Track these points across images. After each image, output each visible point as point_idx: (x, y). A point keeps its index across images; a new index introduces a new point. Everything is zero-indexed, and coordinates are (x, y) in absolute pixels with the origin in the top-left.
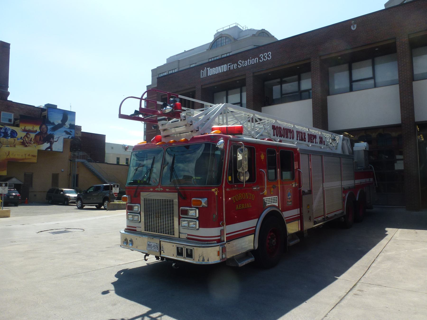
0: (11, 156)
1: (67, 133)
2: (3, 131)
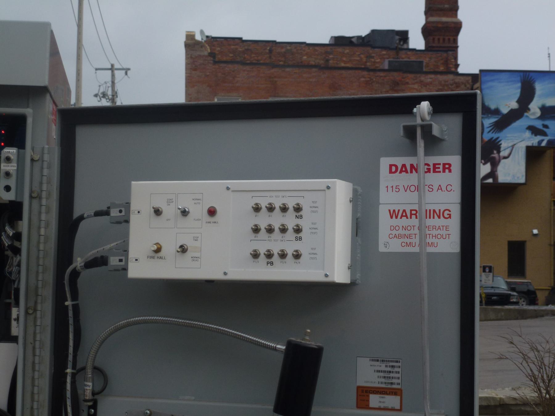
1: (534, 131)
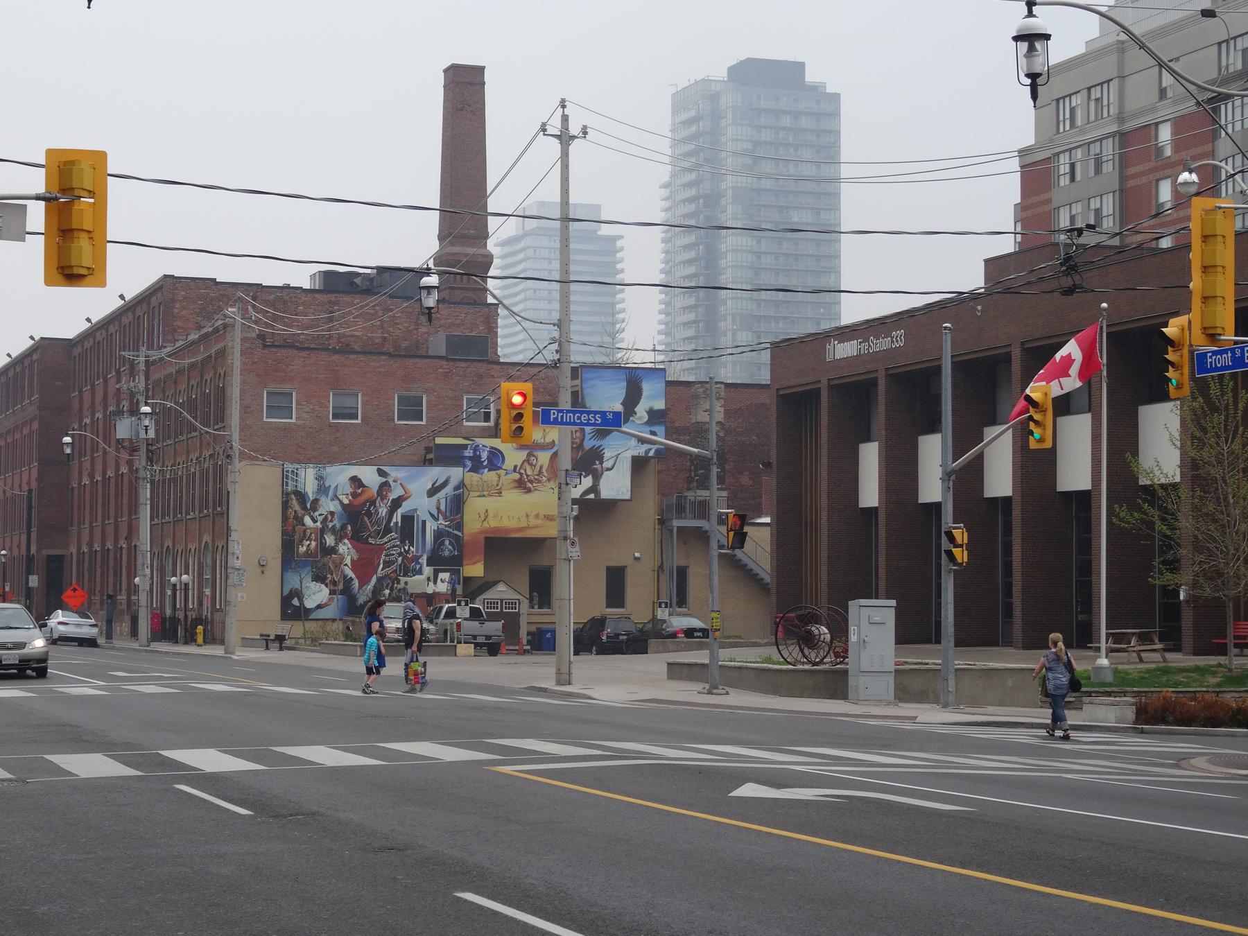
0: (493, 523)
2: (468, 453)
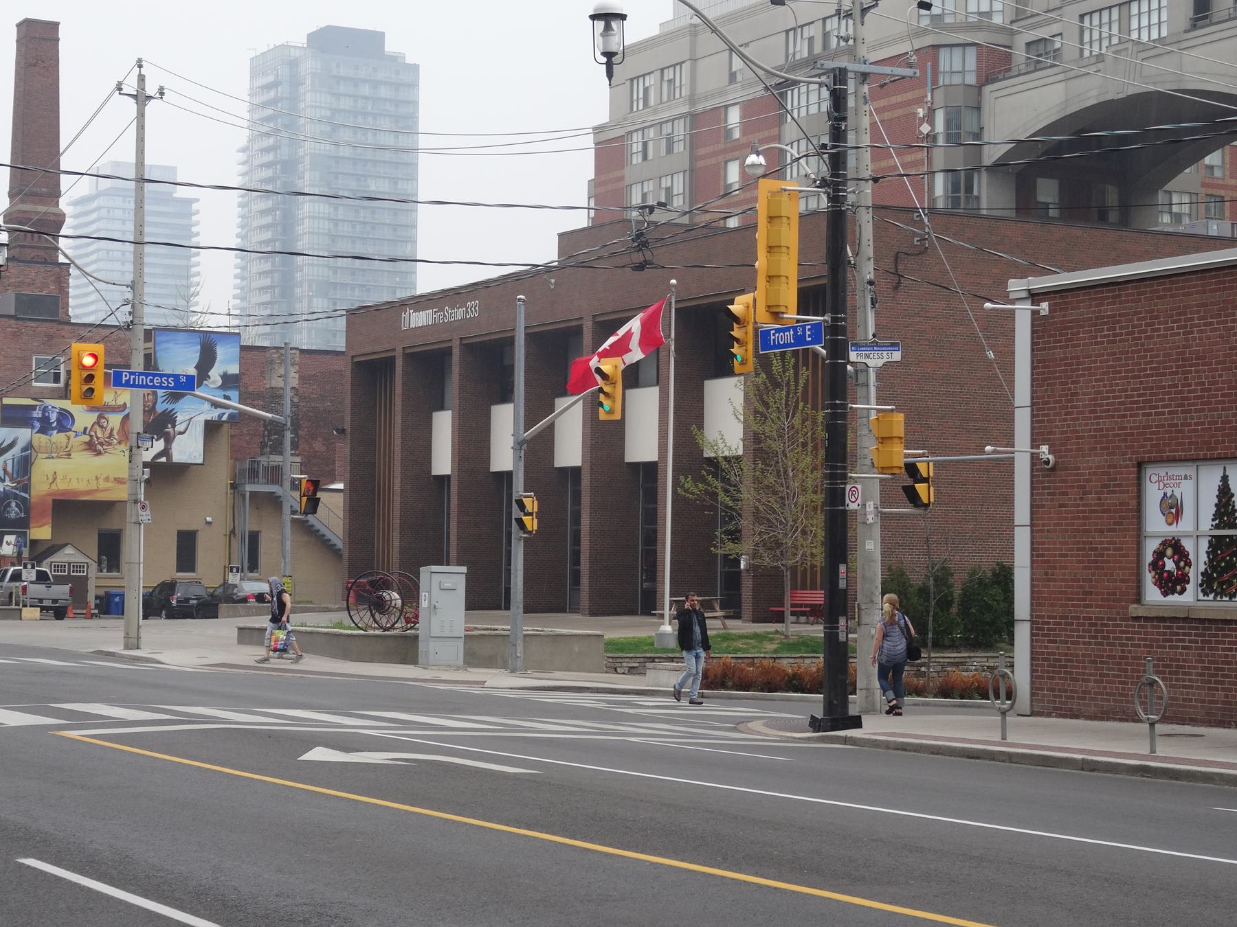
0: (61, 485)
2: (37, 414)
